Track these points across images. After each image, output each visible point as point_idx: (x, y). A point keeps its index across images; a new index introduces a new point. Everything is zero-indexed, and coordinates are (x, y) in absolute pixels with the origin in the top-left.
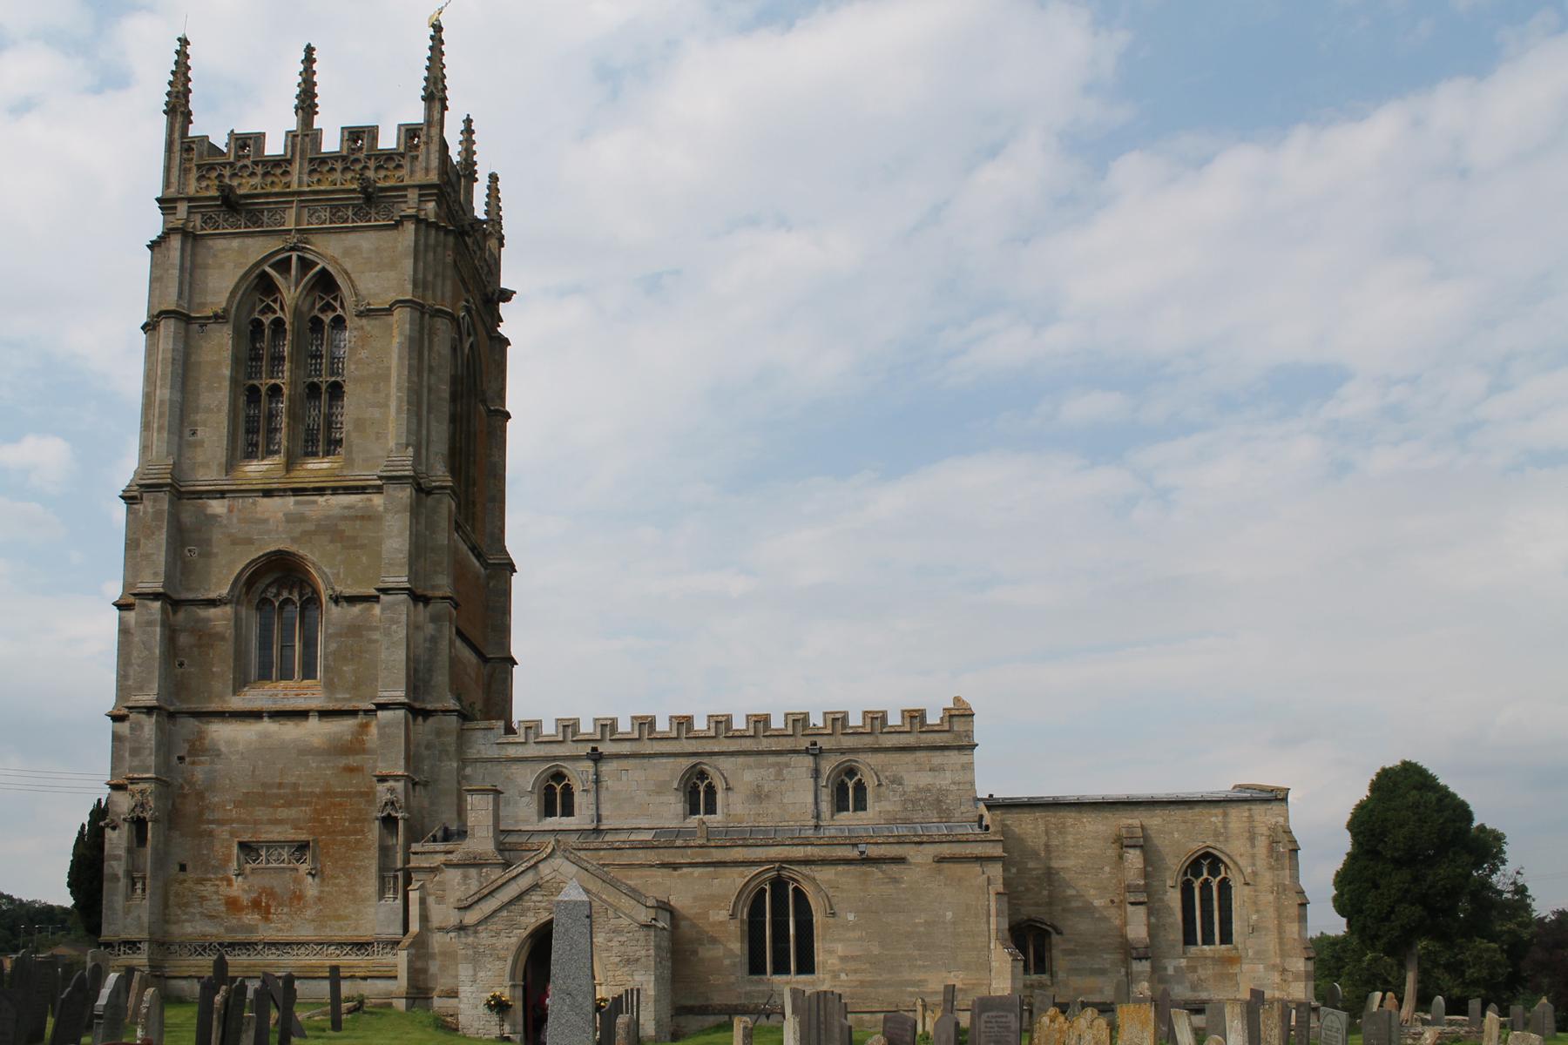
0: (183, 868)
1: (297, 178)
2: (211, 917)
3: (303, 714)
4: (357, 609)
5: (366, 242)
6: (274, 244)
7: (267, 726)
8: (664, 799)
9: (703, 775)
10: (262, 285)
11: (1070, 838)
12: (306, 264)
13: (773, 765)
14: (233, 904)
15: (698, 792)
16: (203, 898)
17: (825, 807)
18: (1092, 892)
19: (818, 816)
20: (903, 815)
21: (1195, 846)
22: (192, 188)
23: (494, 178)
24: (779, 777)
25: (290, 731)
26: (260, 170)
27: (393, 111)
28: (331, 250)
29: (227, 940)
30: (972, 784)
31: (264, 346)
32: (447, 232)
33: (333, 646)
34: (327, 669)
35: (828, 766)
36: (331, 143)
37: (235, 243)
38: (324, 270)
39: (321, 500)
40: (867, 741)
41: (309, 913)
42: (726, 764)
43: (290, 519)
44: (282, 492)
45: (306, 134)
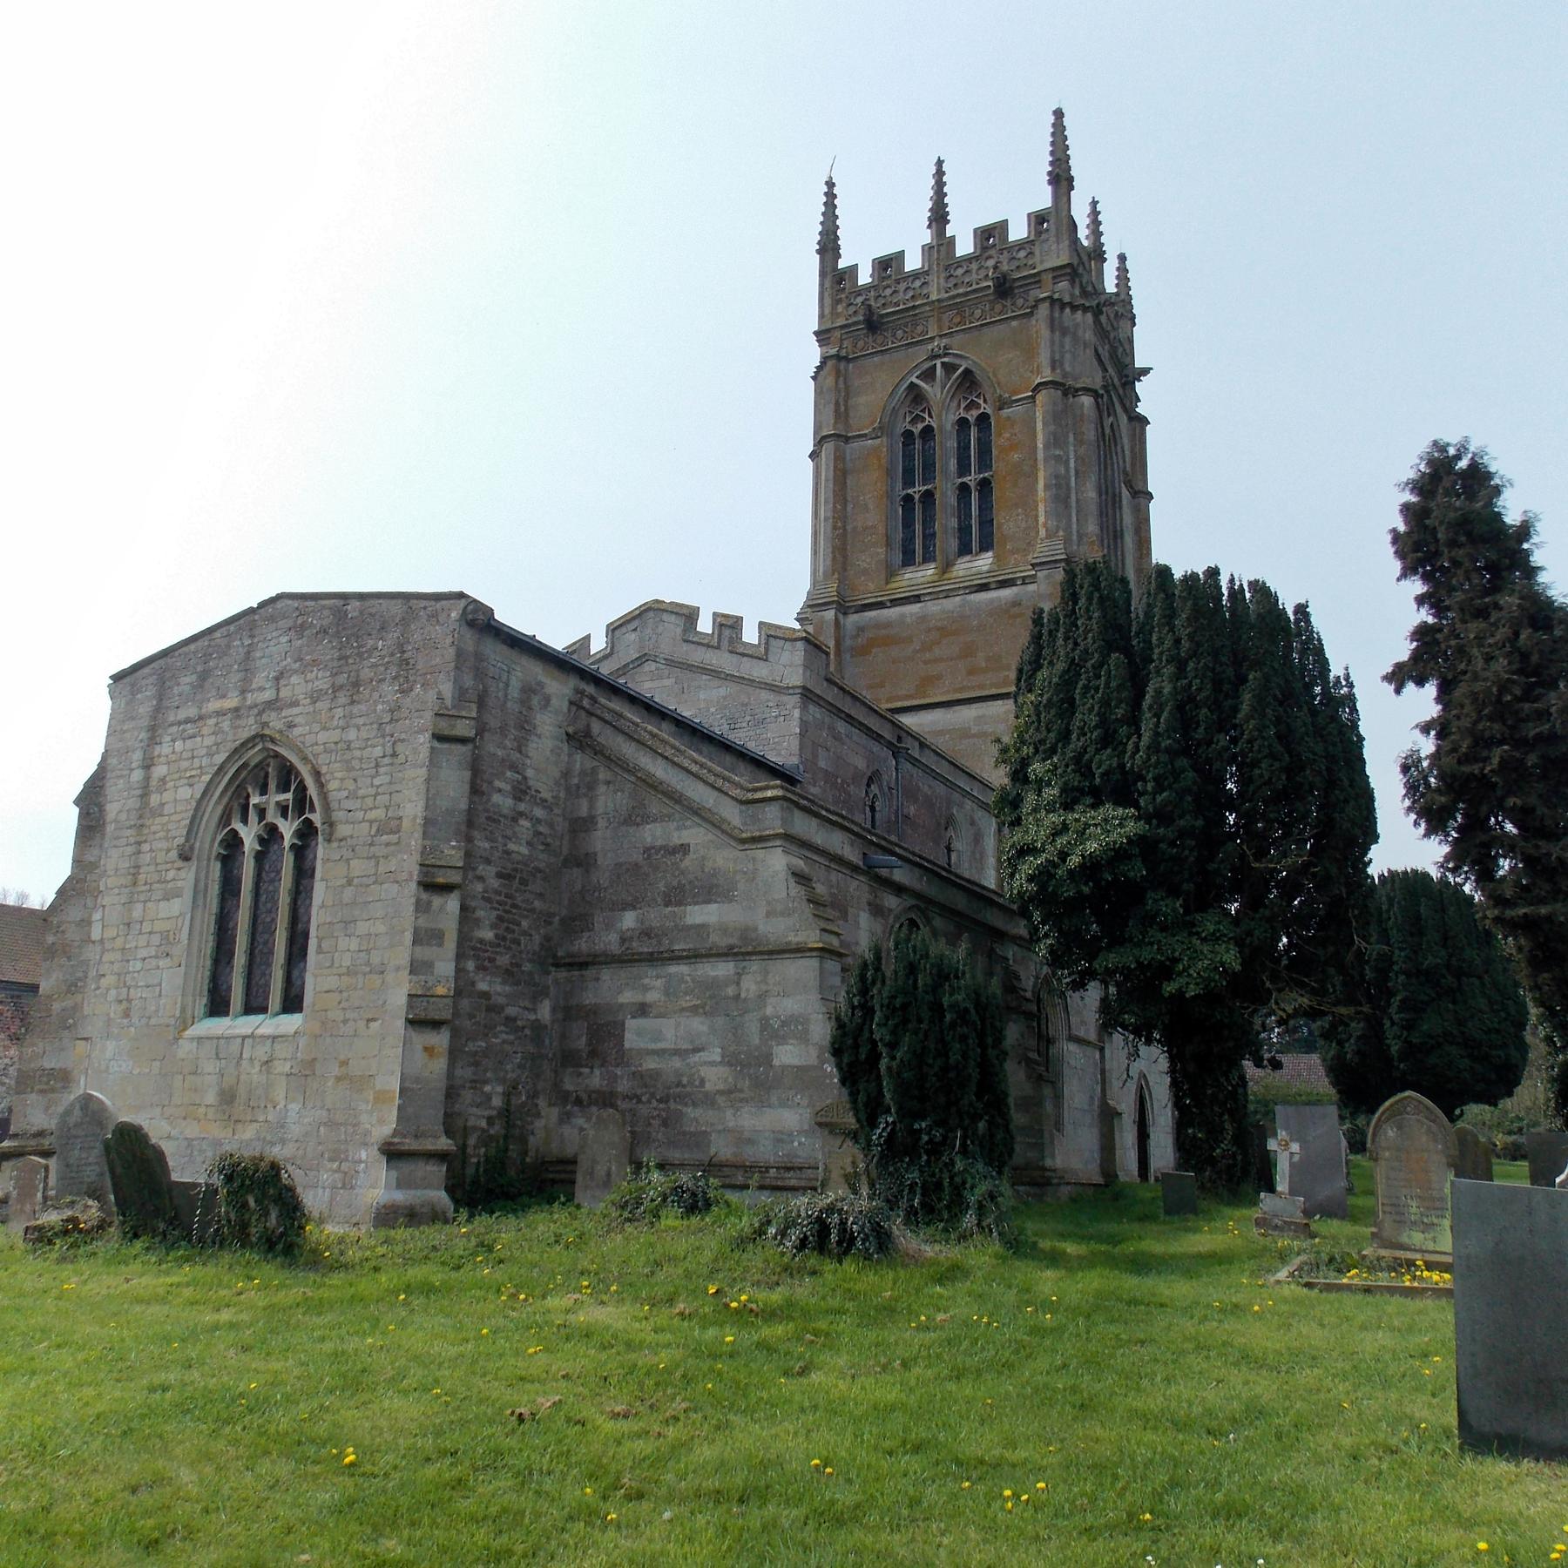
23: (1122, 258)
28: (972, 354)
32: (1085, 309)
36: (965, 246)
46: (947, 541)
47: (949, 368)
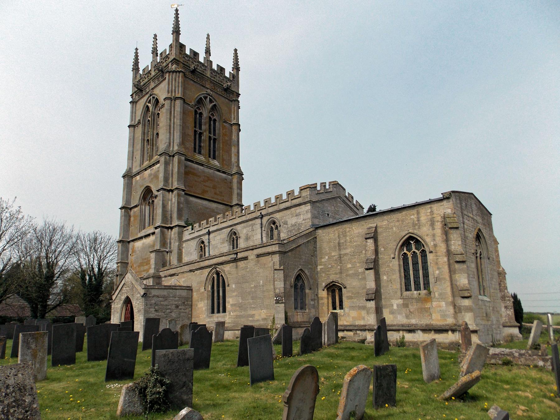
7: (144, 240)
18: (358, 265)
21: (404, 233)
47: (154, 97)
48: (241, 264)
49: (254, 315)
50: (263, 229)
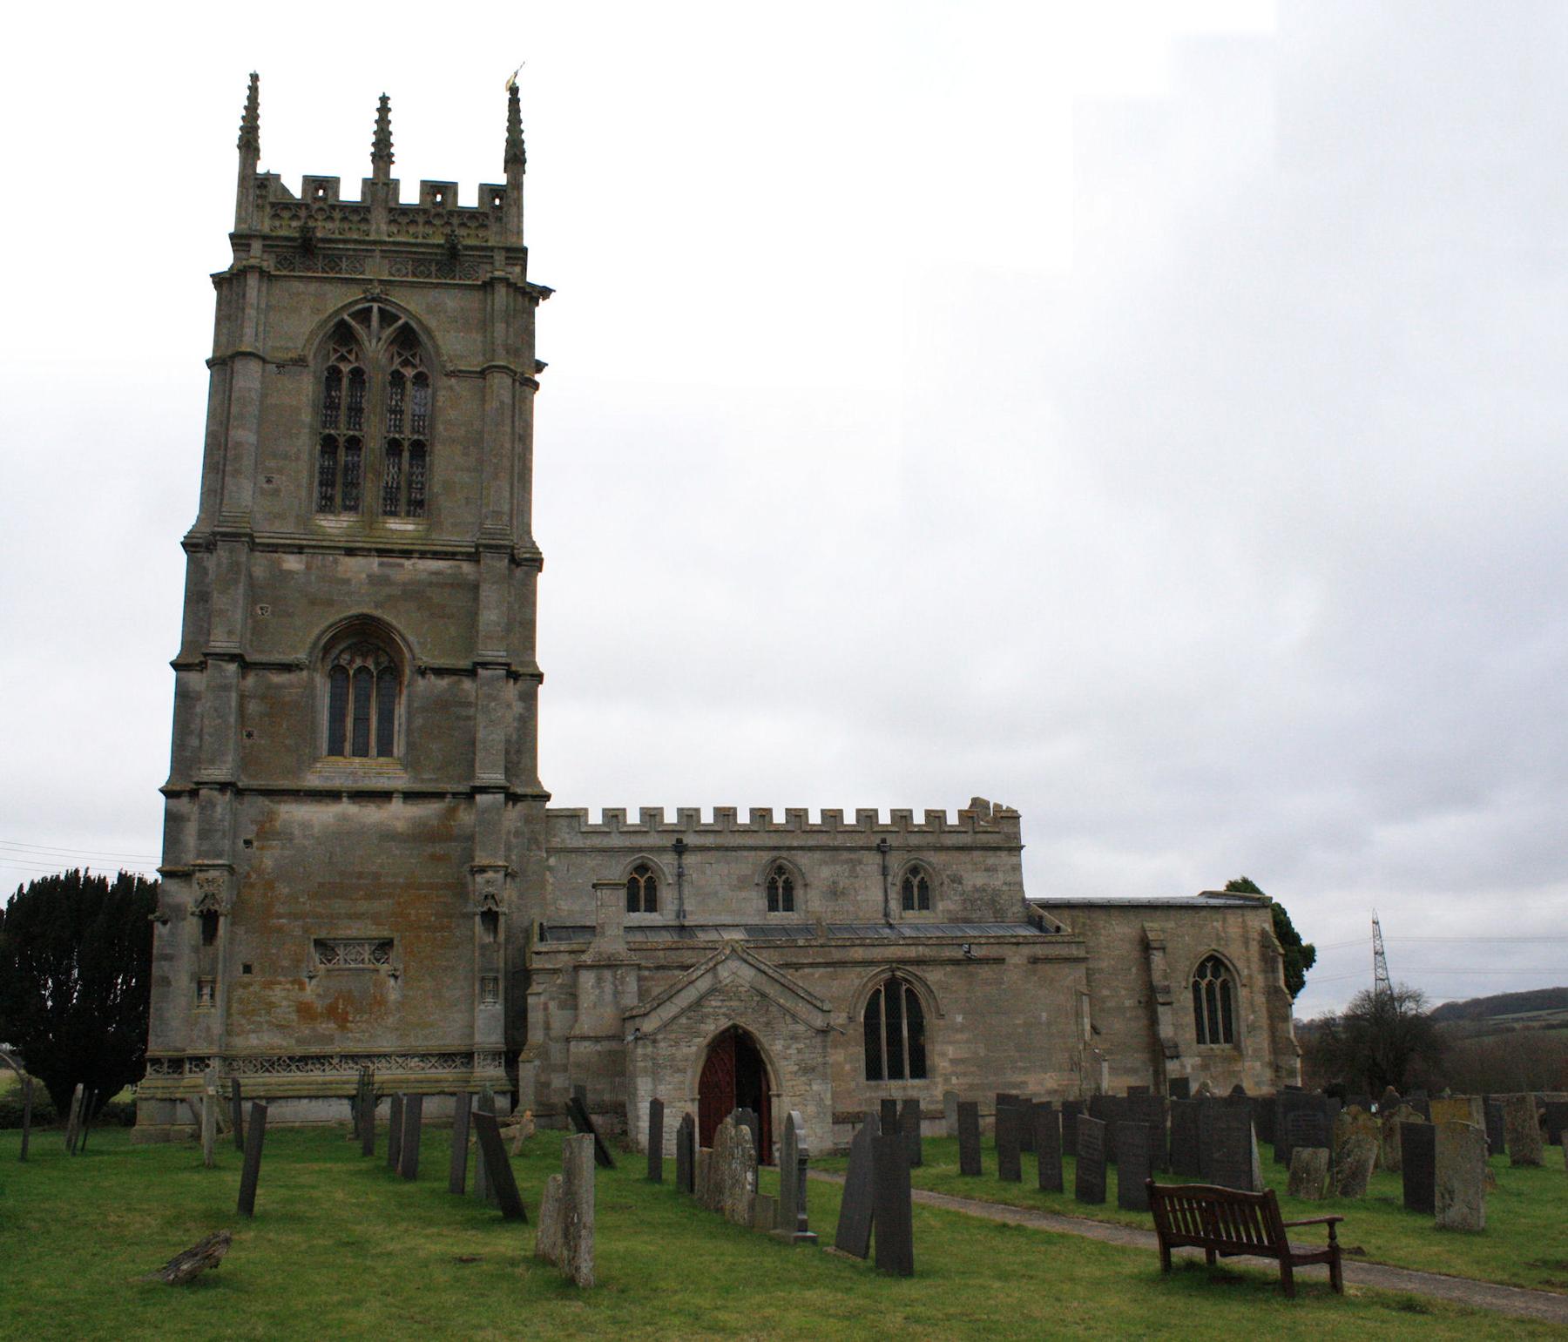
0: (247, 969)
1: (380, 228)
2: (281, 1027)
3: (385, 796)
4: (443, 683)
5: (452, 302)
6: (355, 293)
8: (744, 894)
9: (780, 870)
10: (342, 335)
11: (1102, 939)
12: (387, 318)
13: (846, 862)
14: (305, 1011)
15: (781, 888)
16: (270, 1006)
17: (894, 905)
19: (886, 915)
20: (965, 914)
21: (1204, 951)
22: (266, 226)
24: (853, 874)
25: (372, 814)
26: (337, 215)
27: (473, 171)
28: (413, 304)
29: (299, 1051)
30: (1021, 885)
31: (344, 392)
33: (419, 722)
34: (410, 746)
35: (897, 863)
37: (313, 287)
38: (406, 324)
39: (407, 563)
40: (930, 839)
41: (390, 1020)
42: (804, 860)
43: (373, 580)
44: (366, 552)
45: (381, 185)
46: (371, 492)
48: (985, 972)
49: (1025, 1083)
50: (890, 879)
